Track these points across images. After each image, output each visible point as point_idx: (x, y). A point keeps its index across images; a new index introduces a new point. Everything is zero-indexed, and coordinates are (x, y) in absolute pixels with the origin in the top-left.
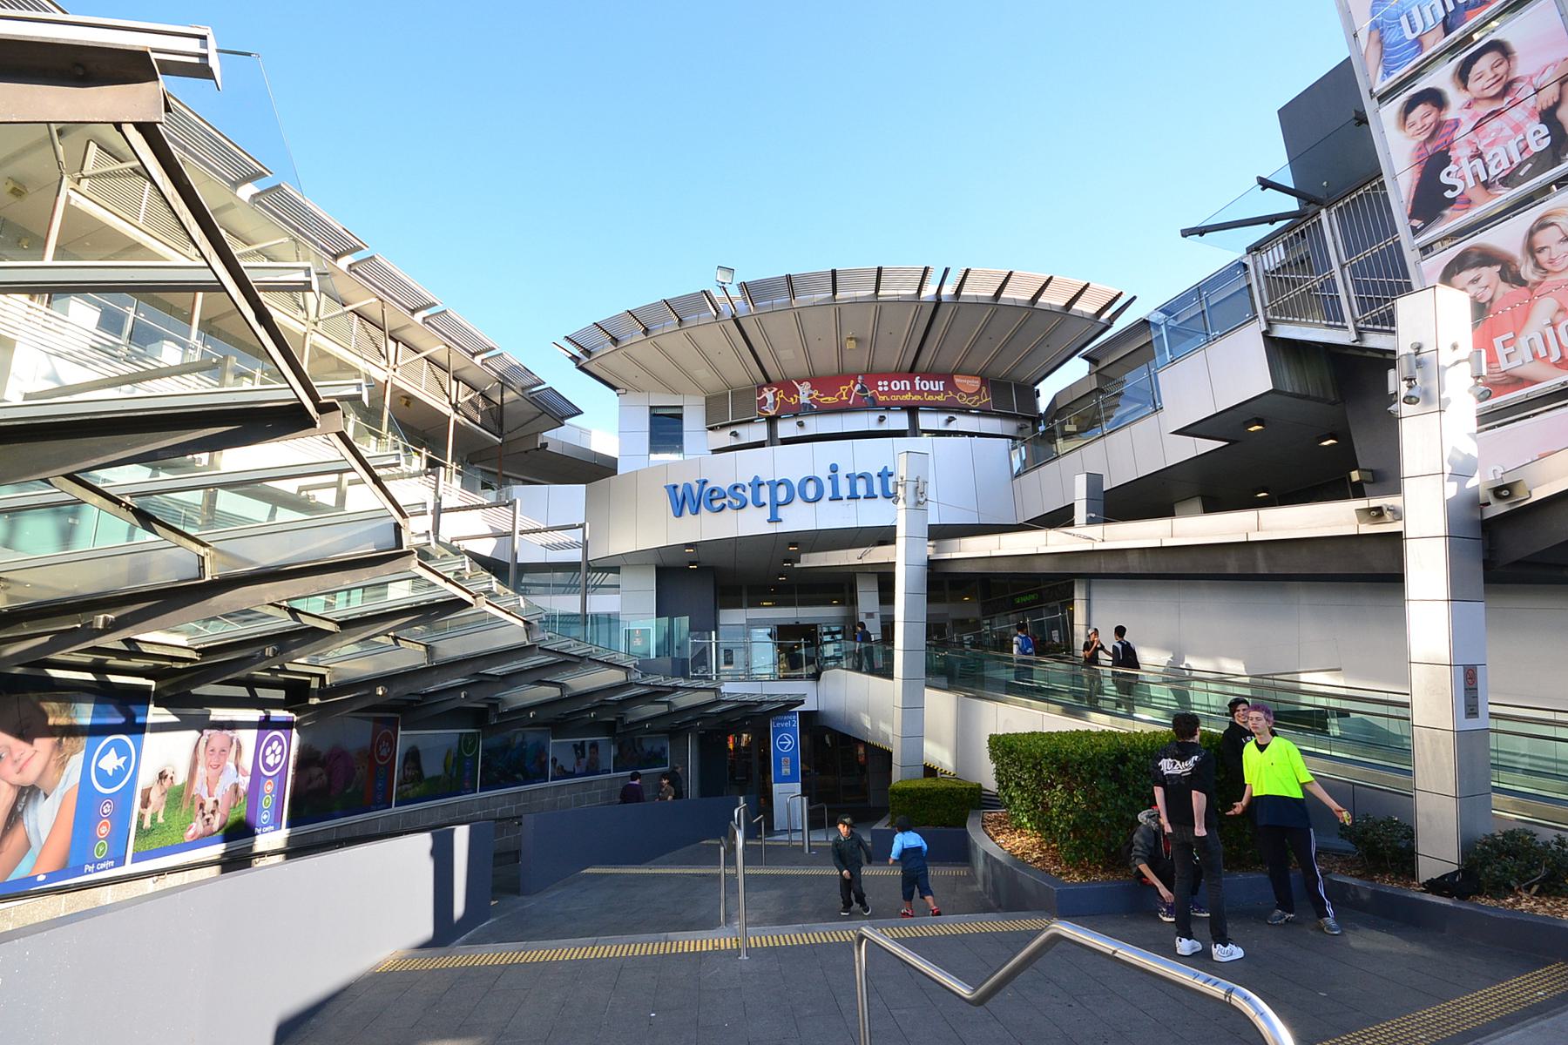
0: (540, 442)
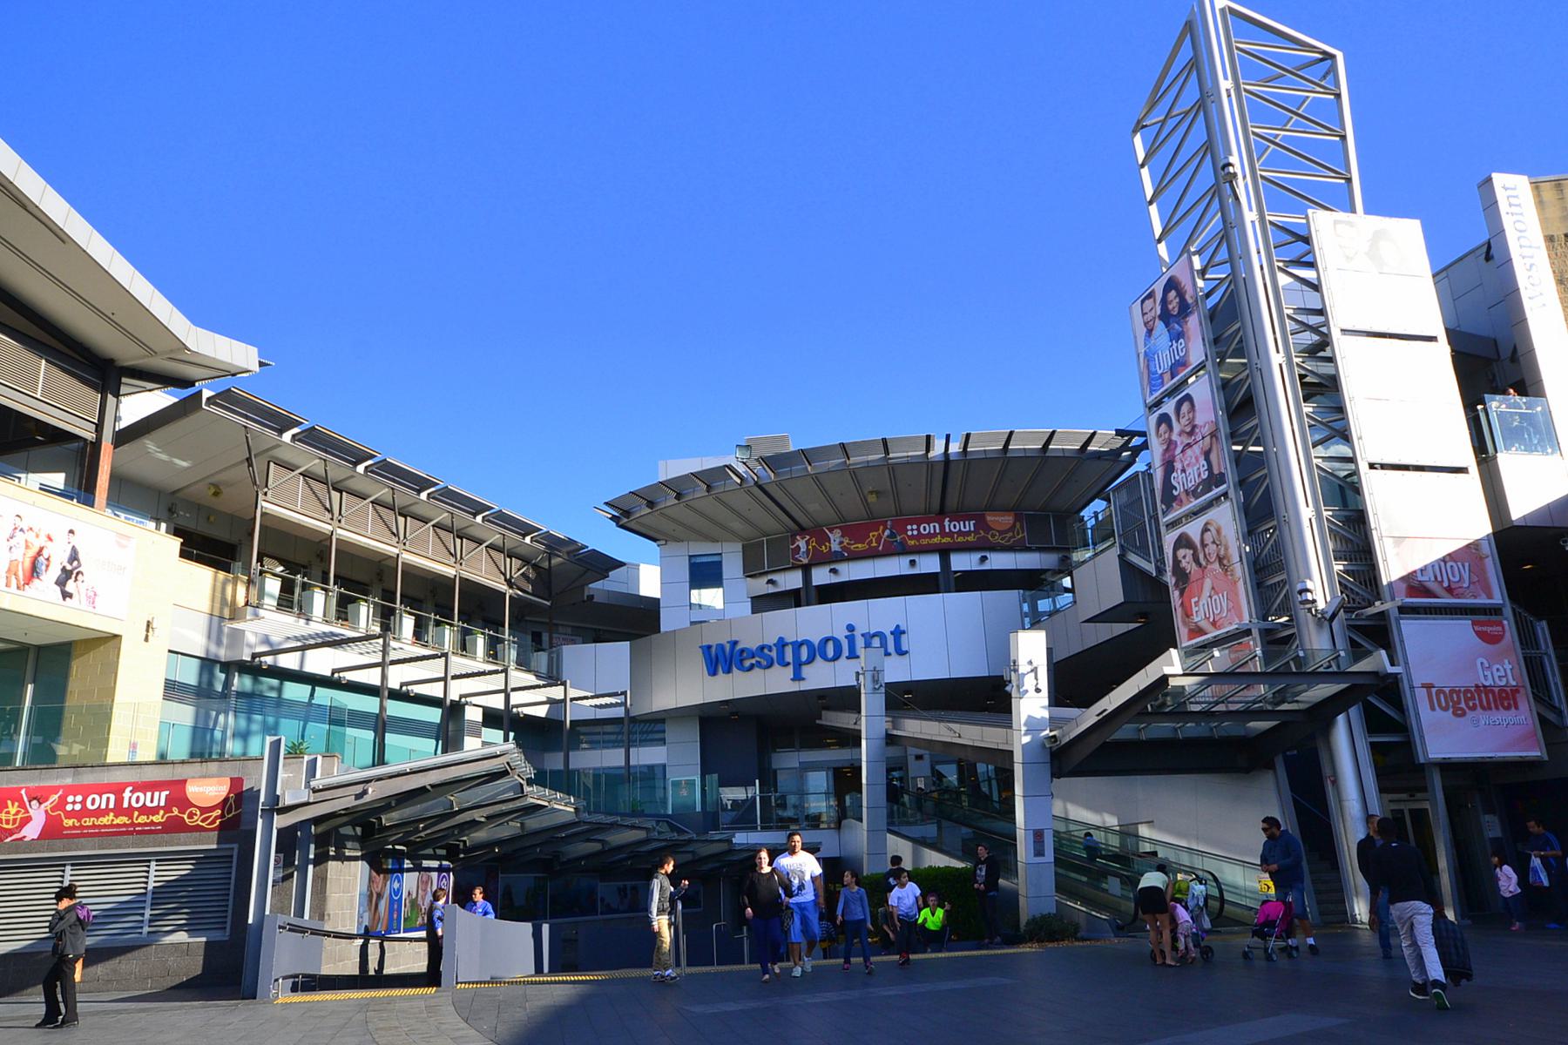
0: (586, 593)
